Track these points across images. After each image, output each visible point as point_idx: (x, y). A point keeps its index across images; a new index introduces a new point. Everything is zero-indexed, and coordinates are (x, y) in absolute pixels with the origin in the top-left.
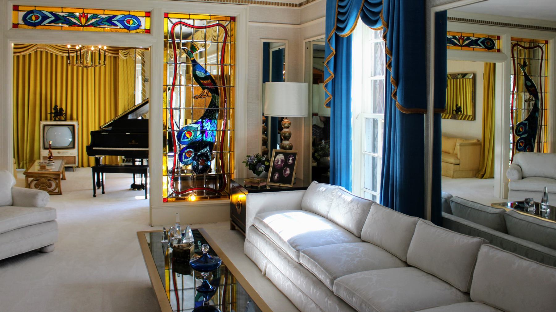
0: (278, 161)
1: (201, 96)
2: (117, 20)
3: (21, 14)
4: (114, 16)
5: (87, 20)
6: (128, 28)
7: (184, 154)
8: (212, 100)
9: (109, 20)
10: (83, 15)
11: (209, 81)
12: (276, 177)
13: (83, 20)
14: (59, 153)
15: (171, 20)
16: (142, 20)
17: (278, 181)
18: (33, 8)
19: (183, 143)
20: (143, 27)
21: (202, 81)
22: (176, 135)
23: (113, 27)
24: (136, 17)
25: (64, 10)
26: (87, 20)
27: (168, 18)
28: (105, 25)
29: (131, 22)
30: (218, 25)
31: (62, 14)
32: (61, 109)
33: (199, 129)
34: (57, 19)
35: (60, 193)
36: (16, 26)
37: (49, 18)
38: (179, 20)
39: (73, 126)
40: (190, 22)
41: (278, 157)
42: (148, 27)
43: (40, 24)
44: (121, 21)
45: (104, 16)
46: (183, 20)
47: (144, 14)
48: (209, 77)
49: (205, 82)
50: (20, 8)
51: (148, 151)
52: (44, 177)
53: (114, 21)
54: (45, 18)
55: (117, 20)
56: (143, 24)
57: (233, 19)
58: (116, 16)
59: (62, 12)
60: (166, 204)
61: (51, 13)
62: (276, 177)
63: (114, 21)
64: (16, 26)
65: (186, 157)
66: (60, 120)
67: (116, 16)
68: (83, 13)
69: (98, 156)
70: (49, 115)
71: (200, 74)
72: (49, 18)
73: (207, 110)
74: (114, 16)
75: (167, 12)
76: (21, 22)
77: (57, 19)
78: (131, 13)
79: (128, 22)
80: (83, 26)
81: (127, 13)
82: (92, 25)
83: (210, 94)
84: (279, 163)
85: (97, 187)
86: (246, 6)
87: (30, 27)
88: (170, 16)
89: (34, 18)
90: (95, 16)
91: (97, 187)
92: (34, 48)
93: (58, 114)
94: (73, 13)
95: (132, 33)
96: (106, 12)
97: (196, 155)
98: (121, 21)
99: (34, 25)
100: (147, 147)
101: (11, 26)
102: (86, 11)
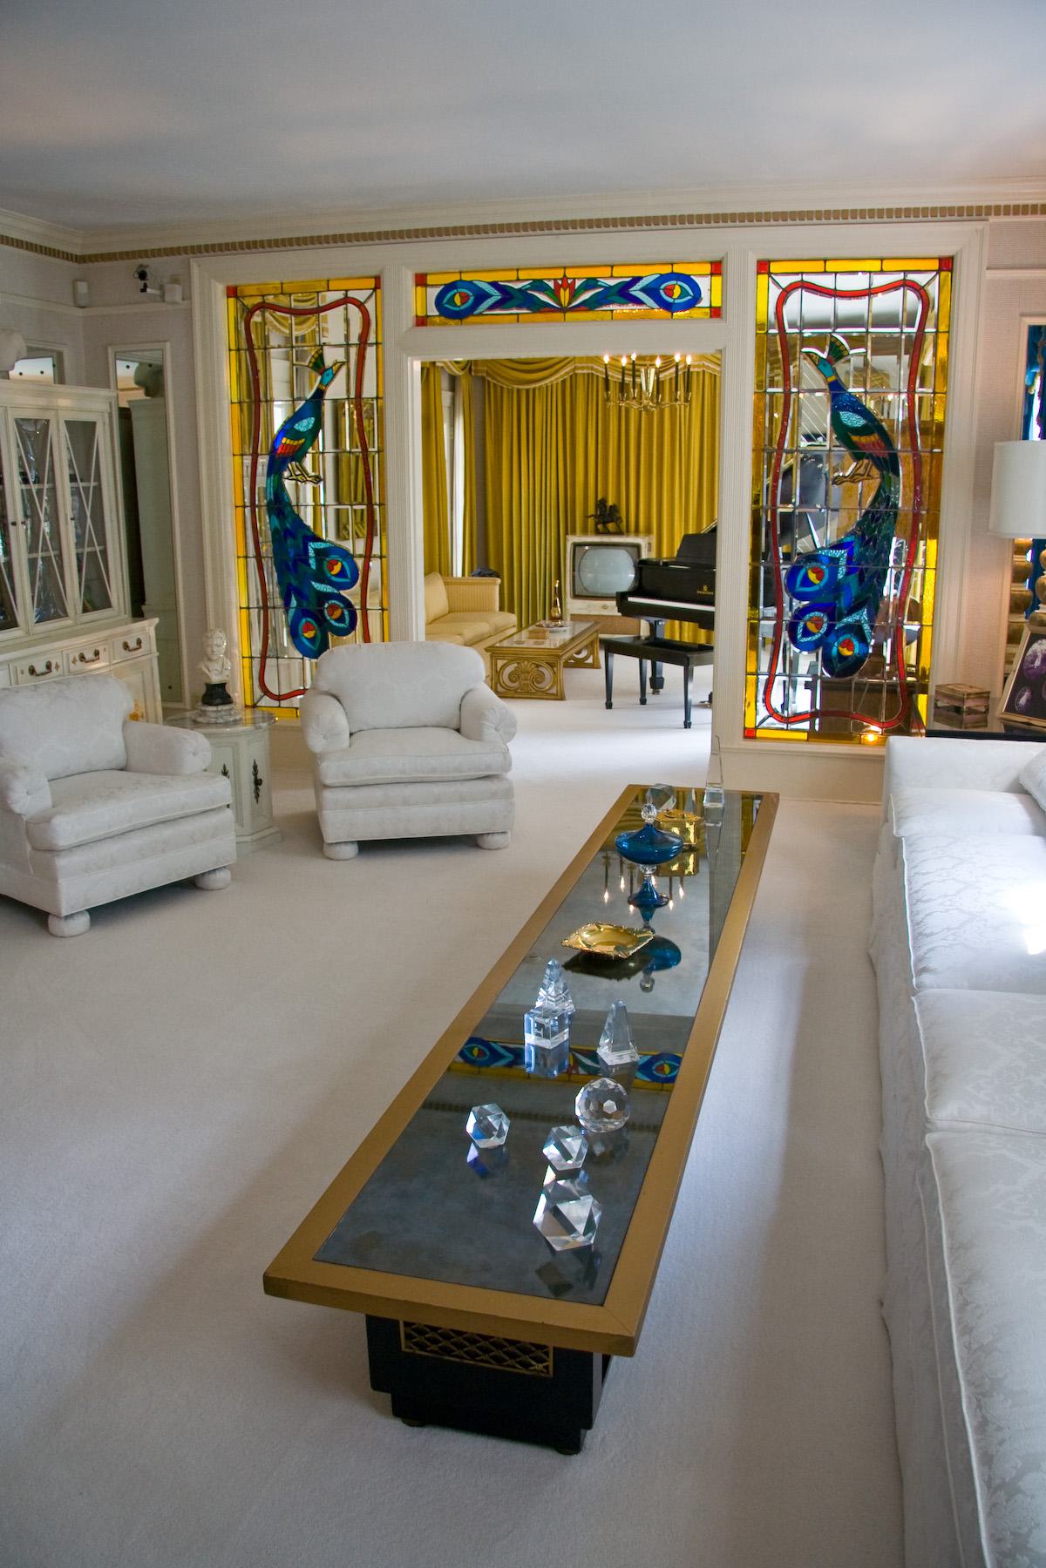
0: (1035, 656)
1: (853, 478)
2: (643, 290)
3: (433, 293)
4: (636, 280)
5: (573, 296)
6: (668, 307)
7: (801, 624)
8: (880, 487)
9: (623, 293)
10: (565, 283)
11: (874, 438)
12: (1023, 701)
13: (565, 295)
14: (605, 607)
15: (777, 278)
16: (703, 283)
17: (1026, 711)
18: (455, 278)
19: (801, 597)
20: (704, 303)
21: (855, 438)
22: (784, 573)
23: (631, 306)
24: (687, 279)
25: (522, 275)
26: (573, 296)
27: (770, 274)
28: (612, 303)
29: (677, 292)
30: (906, 284)
31: (517, 286)
32: (615, 509)
33: (843, 562)
34: (507, 297)
35: (560, 697)
36: (422, 321)
37: (489, 296)
38: (797, 278)
39: (638, 547)
40: (825, 281)
41: (1036, 646)
42: (717, 303)
43: (469, 312)
44: (651, 291)
45: (612, 282)
46: (806, 278)
47: (707, 269)
48: (873, 425)
49: (863, 440)
50: (430, 280)
51: (712, 614)
52: (528, 659)
53: (635, 291)
54: (481, 296)
55: (643, 290)
56: (705, 294)
57: (946, 264)
58: (640, 278)
59: (518, 280)
60: (750, 744)
61: (494, 284)
62: (1023, 701)
63: (635, 291)
64: (422, 321)
65: (806, 633)
66: (608, 533)
67: (640, 278)
68: (565, 278)
69: (653, 619)
70: (591, 522)
71: (852, 420)
72: (489, 296)
73: (867, 513)
74: (636, 280)
75: (762, 257)
76: (433, 311)
77: (507, 297)
78: (678, 269)
79: (669, 292)
80: (563, 310)
81: (667, 270)
82: (588, 306)
83: (875, 472)
84: (1038, 663)
85: (649, 690)
86: (979, 225)
87: (452, 322)
88: (774, 268)
89: (457, 300)
90: (591, 283)
91: (649, 690)
92: (568, 369)
93: (607, 517)
94: (541, 281)
95: (679, 319)
96: (617, 271)
97: (831, 627)
98: (651, 291)
99: (459, 316)
100: (712, 603)
101: (411, 322)
102: (570, 273)
